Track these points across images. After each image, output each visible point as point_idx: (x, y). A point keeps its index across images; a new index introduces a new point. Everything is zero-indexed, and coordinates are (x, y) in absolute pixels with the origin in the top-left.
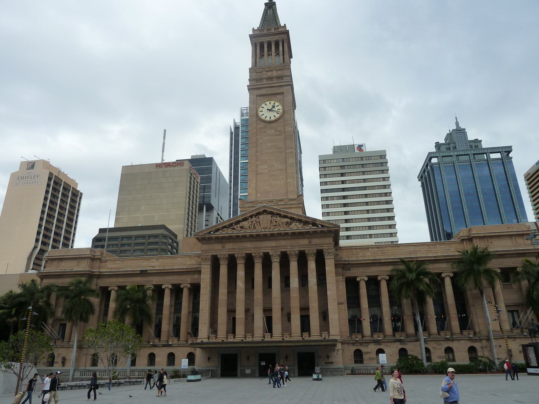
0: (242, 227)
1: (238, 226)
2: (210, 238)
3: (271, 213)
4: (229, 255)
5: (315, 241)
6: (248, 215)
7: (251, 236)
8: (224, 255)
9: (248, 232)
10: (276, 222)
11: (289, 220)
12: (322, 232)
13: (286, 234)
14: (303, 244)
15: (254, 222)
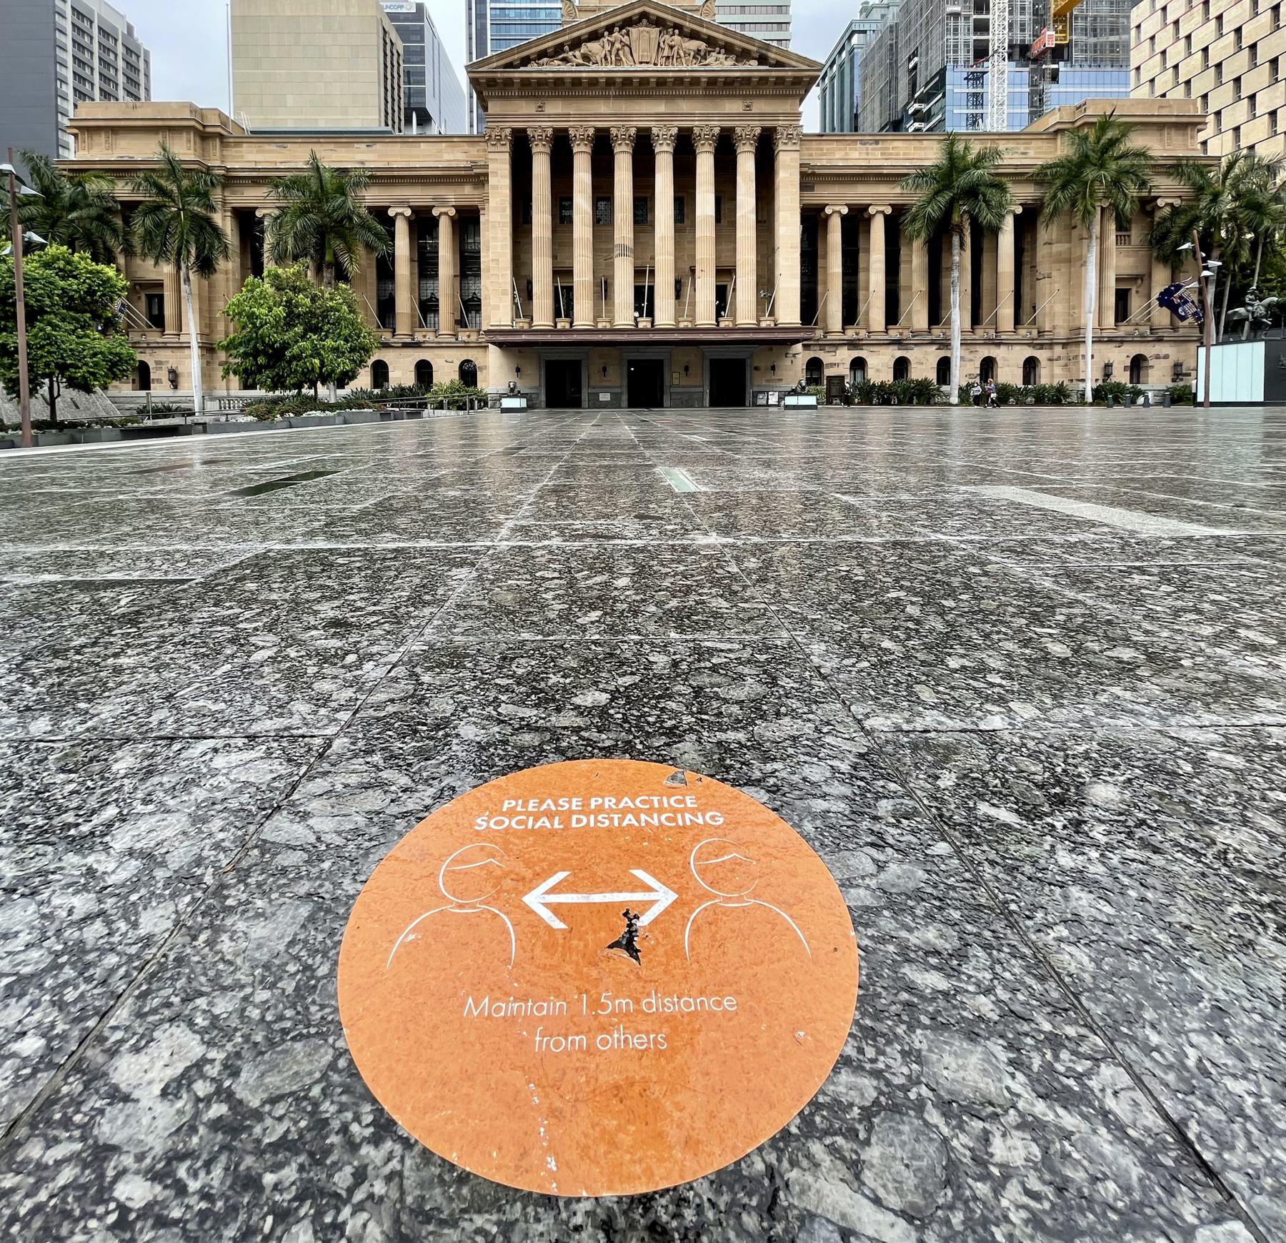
0: (586, 58)
1: (577, 53)
2: (508, 83)
3: (659, 23)
4: (556, 130)
5: (759, 106)
6: (604, 24)
7: (610, 82)
8: (544, 129)
9: (601, 69)
10: (671, 47)
11: (703, 45)
12: (780, 81)
13: (695, 82)
14: (729, 110)
15: (618, 45)
